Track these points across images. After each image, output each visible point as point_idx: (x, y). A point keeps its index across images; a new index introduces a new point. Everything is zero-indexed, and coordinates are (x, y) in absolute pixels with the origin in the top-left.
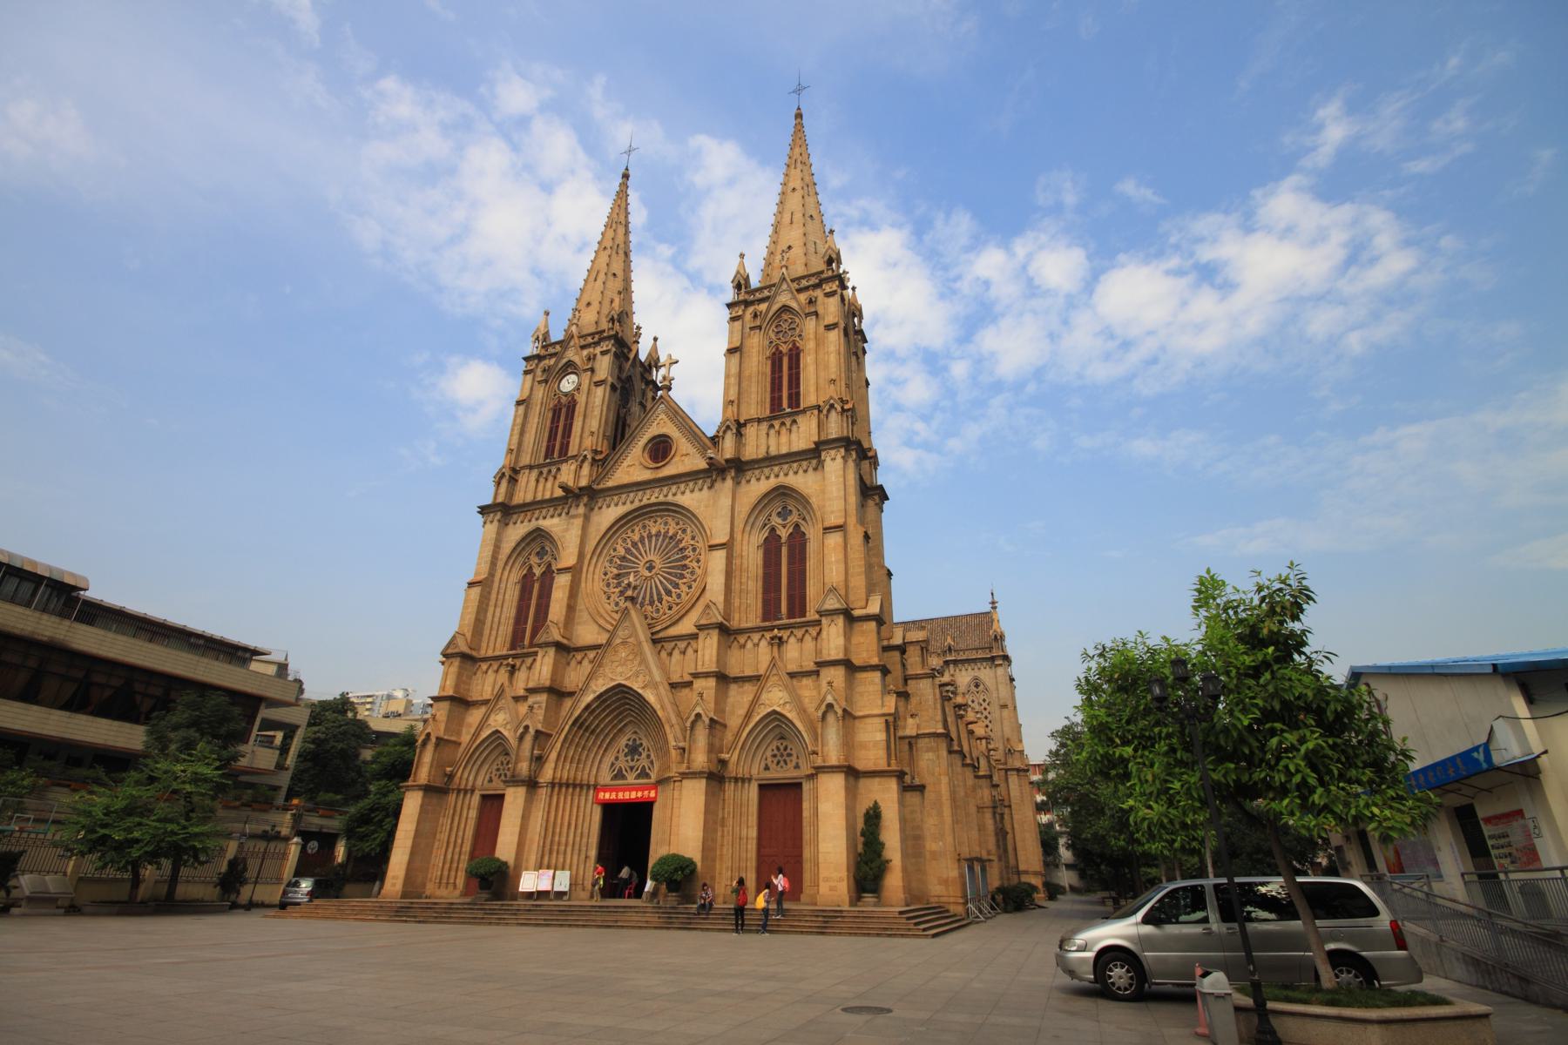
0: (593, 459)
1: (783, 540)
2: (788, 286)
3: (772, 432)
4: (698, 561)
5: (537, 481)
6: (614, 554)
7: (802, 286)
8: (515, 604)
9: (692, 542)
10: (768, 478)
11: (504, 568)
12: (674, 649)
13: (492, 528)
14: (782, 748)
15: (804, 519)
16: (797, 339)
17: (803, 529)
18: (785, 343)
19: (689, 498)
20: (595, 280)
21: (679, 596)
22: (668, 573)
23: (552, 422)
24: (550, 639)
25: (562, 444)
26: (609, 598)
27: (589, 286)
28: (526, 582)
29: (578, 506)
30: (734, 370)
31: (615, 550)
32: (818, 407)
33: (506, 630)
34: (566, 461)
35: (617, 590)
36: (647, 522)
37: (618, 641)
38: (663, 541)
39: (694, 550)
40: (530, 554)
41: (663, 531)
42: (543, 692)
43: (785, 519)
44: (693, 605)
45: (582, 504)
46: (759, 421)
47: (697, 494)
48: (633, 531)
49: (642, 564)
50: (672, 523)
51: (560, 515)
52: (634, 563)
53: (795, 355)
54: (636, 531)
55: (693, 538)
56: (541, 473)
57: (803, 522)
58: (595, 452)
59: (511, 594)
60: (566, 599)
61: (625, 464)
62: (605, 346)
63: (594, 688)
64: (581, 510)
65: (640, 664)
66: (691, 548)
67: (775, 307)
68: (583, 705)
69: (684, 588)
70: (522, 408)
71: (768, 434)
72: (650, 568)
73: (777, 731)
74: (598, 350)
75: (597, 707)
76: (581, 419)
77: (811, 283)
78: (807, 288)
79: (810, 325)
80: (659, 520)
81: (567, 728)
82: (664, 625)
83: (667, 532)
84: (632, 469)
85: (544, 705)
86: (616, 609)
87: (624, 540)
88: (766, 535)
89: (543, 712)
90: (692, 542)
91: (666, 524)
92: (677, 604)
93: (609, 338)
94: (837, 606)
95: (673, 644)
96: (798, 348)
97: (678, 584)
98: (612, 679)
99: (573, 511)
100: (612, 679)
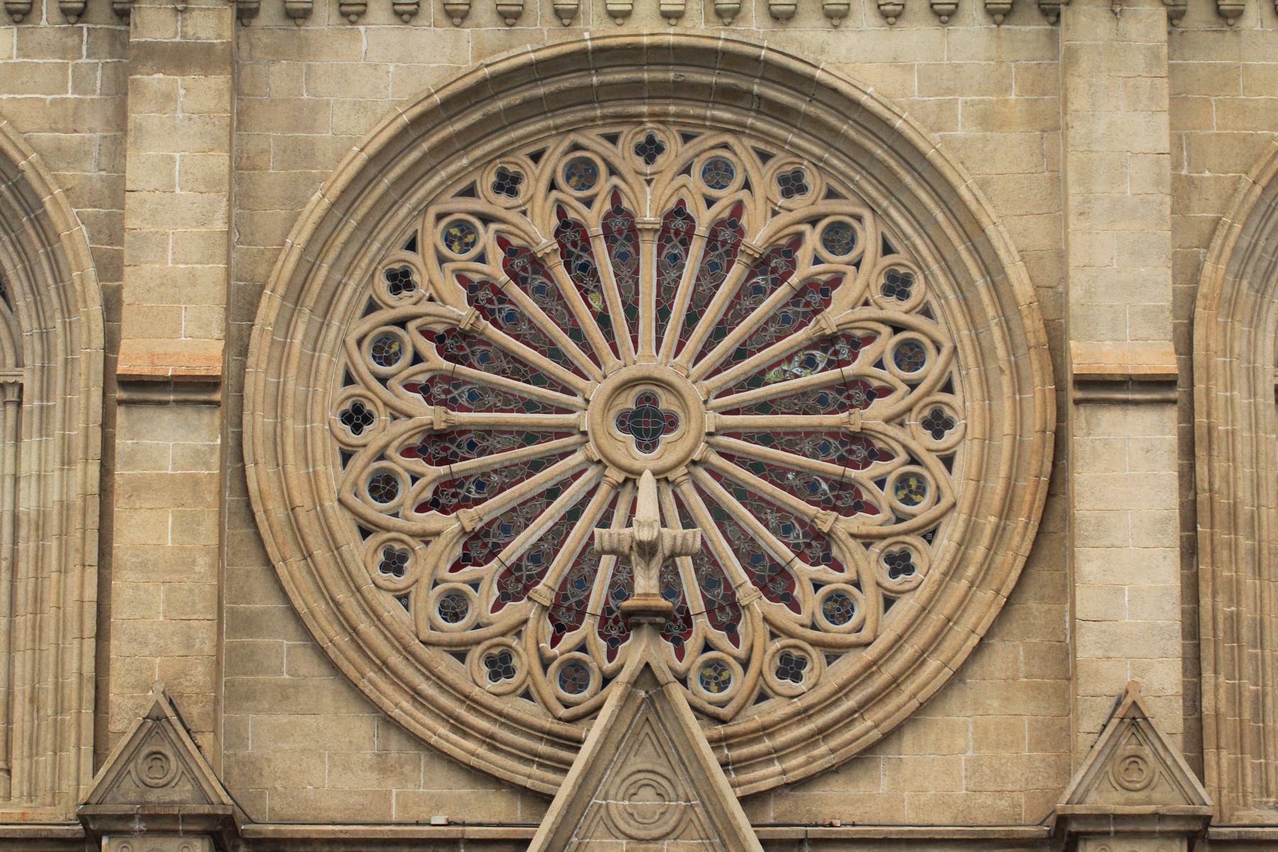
4: (938, 423)
6: (403, 304)
9: (895, 309)
21: (839, 606)
22: (757, 467)
24: (180, 795)
26: (394, 563)
31: (400, 281)
35: (449, 525)
36: (592, 139)
38: (713, 272)
41: (704, 219)
44: (959, 675)
48: (508, 184)
49: (597, 390)
50: (765, 181)
52: (538, 378)
54: (534, 181)
55: (897, 285)
60: (203, 563)
66: (887, 343)
69: (871, 565)
82: (796, 765)
83: (733, 221)
86: (456, 631)
87: (460, 235)
90: (895, 309)
91: (718, 173)
92: (833, 652)
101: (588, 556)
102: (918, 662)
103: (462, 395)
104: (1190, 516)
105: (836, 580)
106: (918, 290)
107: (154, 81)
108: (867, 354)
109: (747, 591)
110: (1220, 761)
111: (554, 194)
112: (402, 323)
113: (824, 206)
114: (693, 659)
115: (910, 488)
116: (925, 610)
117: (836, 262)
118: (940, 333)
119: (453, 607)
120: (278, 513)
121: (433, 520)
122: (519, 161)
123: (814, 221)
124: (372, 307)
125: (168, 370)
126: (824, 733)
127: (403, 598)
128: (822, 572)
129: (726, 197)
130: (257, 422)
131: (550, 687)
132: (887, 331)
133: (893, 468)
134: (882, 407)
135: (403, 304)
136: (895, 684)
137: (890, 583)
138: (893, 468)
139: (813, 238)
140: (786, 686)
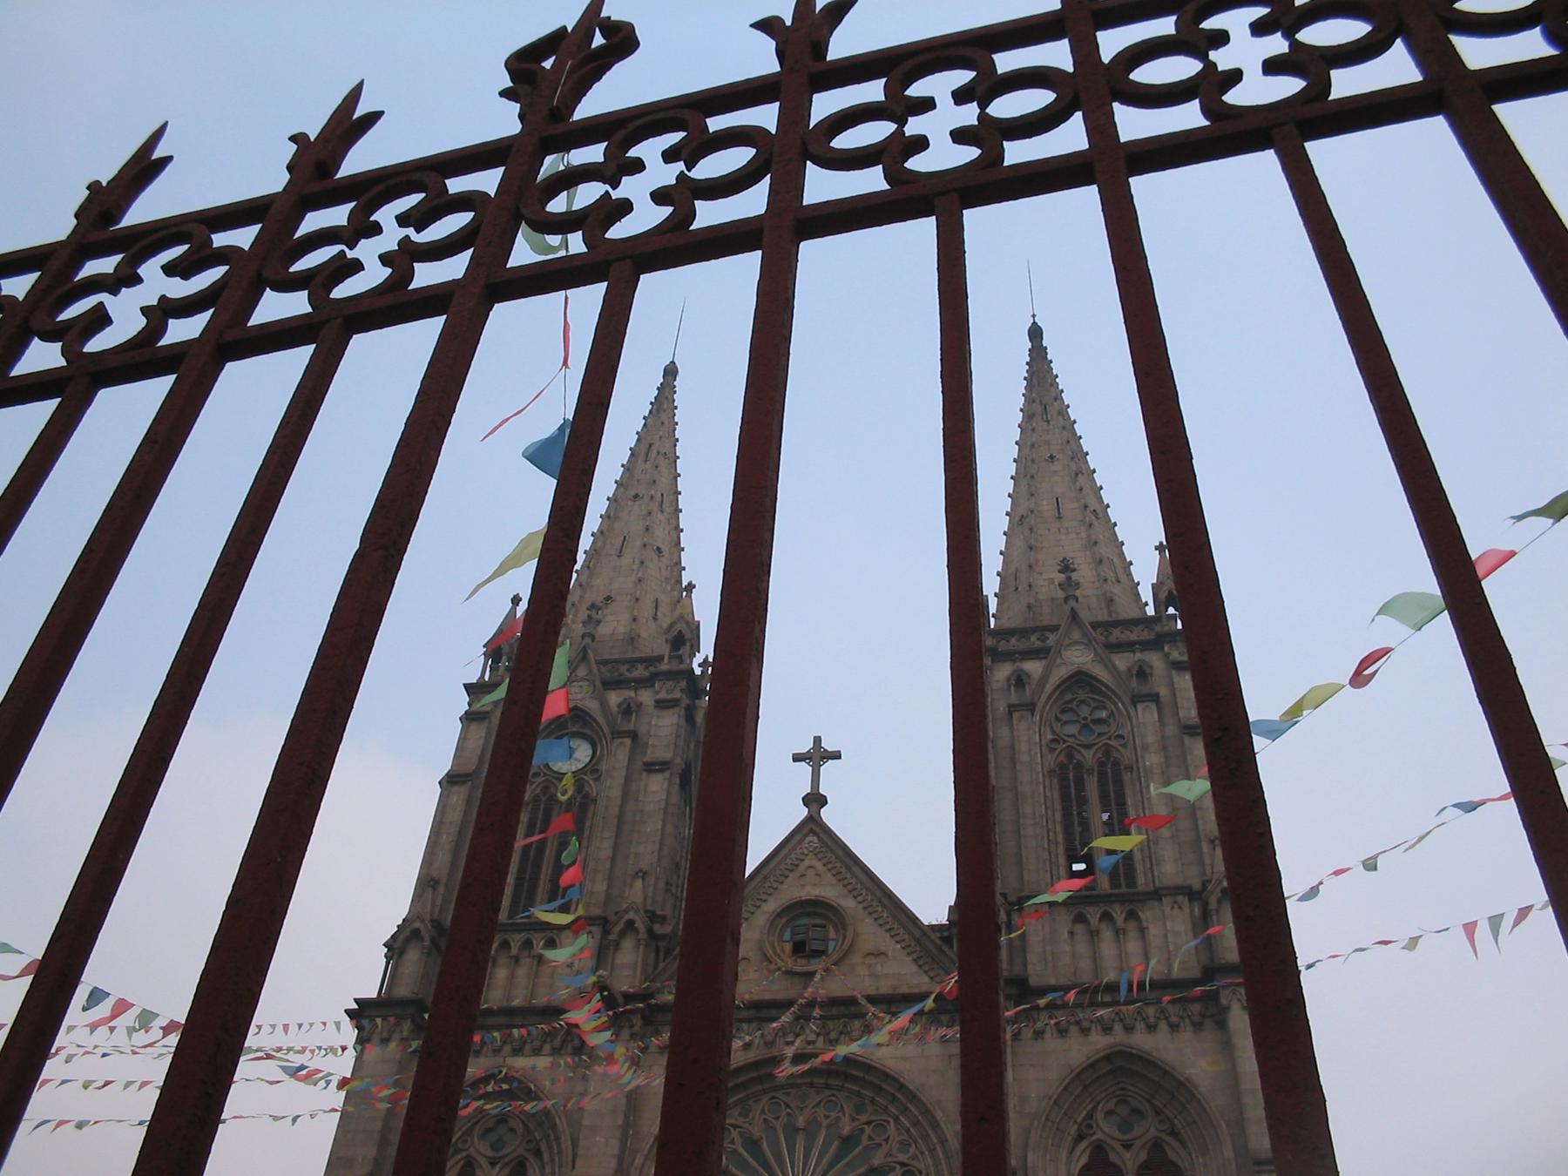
0: (650, 932)
2: (1085, 634)
3: (1079, 928)
7: (1112, 639)
10: (1085, 1032)
15: (1174, 1133)
17: (1172, 1156)
18: (1088, 747)
32: (1193, 895)
55: (904, 1146)
57: (1170, 1139)
58: (653, 917)
62: (664, 690)
67: (1060, 673)
71: (1071, 933)
74: (646, 697)
76: (609, 834)
77: (1133, 637)
78: (1128, 646)
79: (1147, 716)
88: (1084, 1160)
90: (902, 1157)
93: (670, 675)
96: (1116, 763)
111: (764, 1116)
113: (873, 1118)
118: (922, 1166)
123: (868, 1123)
129: (833, 1115)
132: (898, 1167)
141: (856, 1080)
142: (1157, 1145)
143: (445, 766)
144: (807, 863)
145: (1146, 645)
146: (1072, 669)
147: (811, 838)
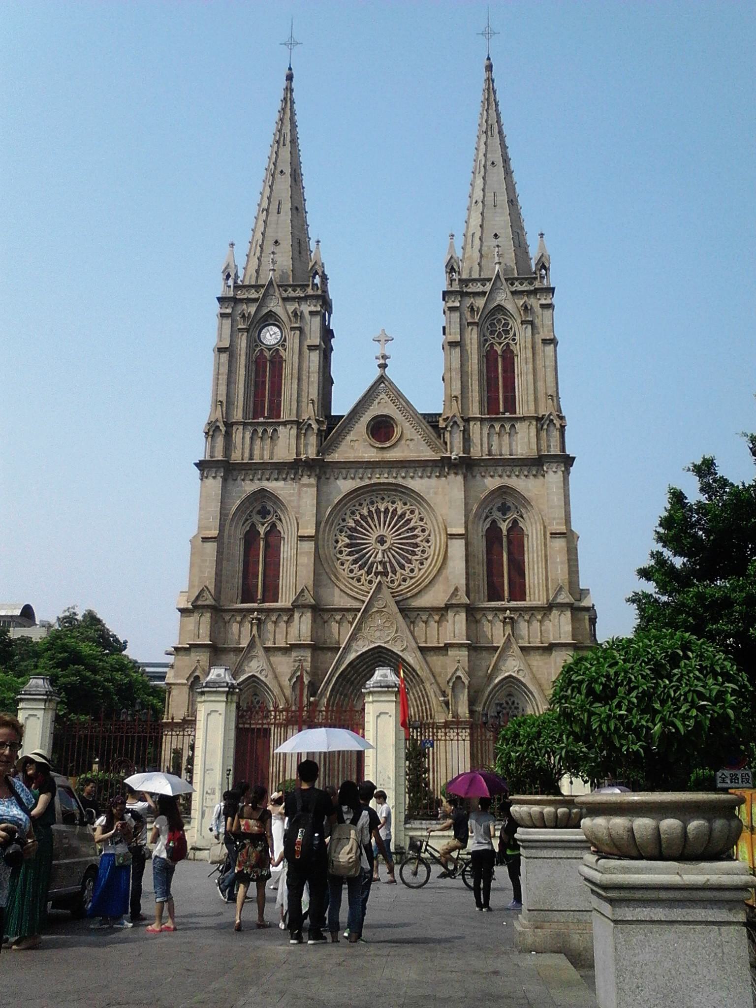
0: (319, 429)
1: (505, 532)
4: (428, 541)
5: (252, 438)
6: (344, 524)
8: (242, 558)
9: (422, 523)
11: (231, 526)
12: (416, 618)
13: (215, 484)
14: (510, 703)
15: (522, 517)
16: (511, 342)
17: (521, 525)
18: (500, 344)
19: (416, 484)
20: (279, 213)
21: (412, 571)
23: (257, 376)
25: (271, 402)
27: (273, 217)
28: (251, 537)
29: (309, 476)
30: (456, 364)
31: (344, 520)
32: (538, 419)
33: (238, 581)
34: (285, 424)
37: (375, 610)
38: (392, 518)
39: (423, 531)
40: (251, 512)
42: (308, 647)
43: (504, 514)
45: (313, 474)
46: (482, 420)
47: (426, 481)
48: (361, 505)
51: (285, 479)
53: (509, 357)
55: (421, 519)
56: (255, 431)
57: (522, 520)
59: (238, 550)
60: (312, 565)
61: (349, 438)
63: (356, 647)
64: (313, 481)
65: (396, 632)
66: (420, 529)
68: (347, 662)
70: (224, 357)
72: (381, 540)
73: (508, 689)
75: (358, 664)
80: (387, 499)
81: (334, 679)
83: (395, 510)
84: (356, 444)
85: (309, 659)
86: (352, 575)
88: (488, 526)
89: (309, 664)
91: (393, 503)
92: (411, 578)
94: (567, 600)
95: (416, 613)
96: (512, 352)
97: (410, 560)
98: (371, 641)
99: (305, 480)
100: (371, 641)
101: (372, 564)
102: (424, 581)
103: (353, 538)
104: (467, 556)
105: (412, 566)
106: (425, 521)
107: (305, 489)
108: (417, 530)
109: (398, 568)
110: (472, 596)
112: (344, 527)
114: (389, 579)
115: (423, 552)
116: (426, 571)
117: (412, 516)
119: (351, 571)
120: (324, 556)
121: (348, 558)
122: (362, 502)
123: (408, 510)
124: (339, 524)
125: (306, 535)
126: (409, 591)
127: (344, 570)
128: (409, 565)
130: (320, 543)
131: (366, 583)
133: (421, 549)
134: (419, 539)
135: (344, 524)
136: (420, 584)
137: (421, 567)
138: (421, 549)
139: (408, 512)
140: (404, 583)
141: (403, 493)
142: (515, 522)
143: (212, 341)
144: (381, 396)
145: (529, 293)
146: (496, 304)
147: (382, 385)
